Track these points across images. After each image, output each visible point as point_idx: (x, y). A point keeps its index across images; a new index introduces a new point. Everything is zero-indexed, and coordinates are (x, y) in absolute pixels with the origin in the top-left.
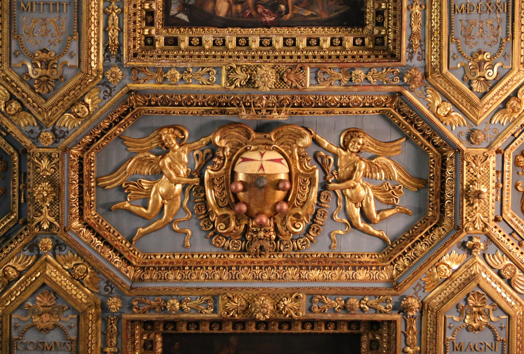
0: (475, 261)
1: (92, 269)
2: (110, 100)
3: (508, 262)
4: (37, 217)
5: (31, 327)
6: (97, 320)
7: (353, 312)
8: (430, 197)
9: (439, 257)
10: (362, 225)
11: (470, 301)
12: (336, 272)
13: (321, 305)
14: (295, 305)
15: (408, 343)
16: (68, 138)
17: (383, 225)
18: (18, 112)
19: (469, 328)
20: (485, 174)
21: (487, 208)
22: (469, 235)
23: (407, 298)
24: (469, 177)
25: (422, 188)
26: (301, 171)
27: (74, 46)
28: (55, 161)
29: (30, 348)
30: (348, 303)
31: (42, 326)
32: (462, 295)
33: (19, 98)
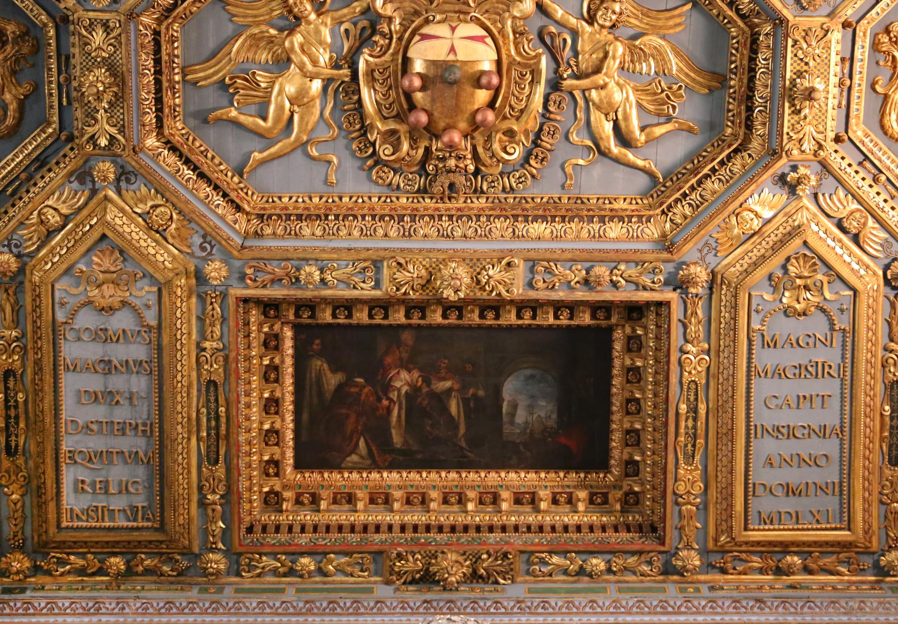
0: (801, 204)
1: (180, 213)
3: (855, 206)
4: (89, 126)
5: (84, 305)
6: (189, 297)
7: (599, 288)
8: (729, 103)
9: (741, 199)
10: (616, 149)
11: (791, 268)
12: (573, 225)
13: (547, 277)
14: (506, 276)
15: (688, 337)
17: (650, 151)
19: (787, 312)
20: (823, 61)
21: (823, 117)
22: (792, 163)
23: (688, 265)
24: (795, 65)
25: (717, 88)
26: (518, 59)
29: (85, 337)
30: (592, 273)
31: (104, 303)
32: (779, 259)
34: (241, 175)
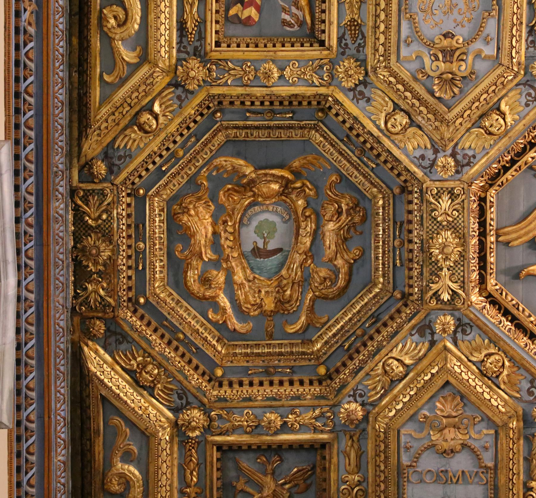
4: (433, 283)
5: (427, 449)
6: (519, 439)
16: (475, 165)
28: (459, 200)
29: (428, 479)
31: (446, 446)
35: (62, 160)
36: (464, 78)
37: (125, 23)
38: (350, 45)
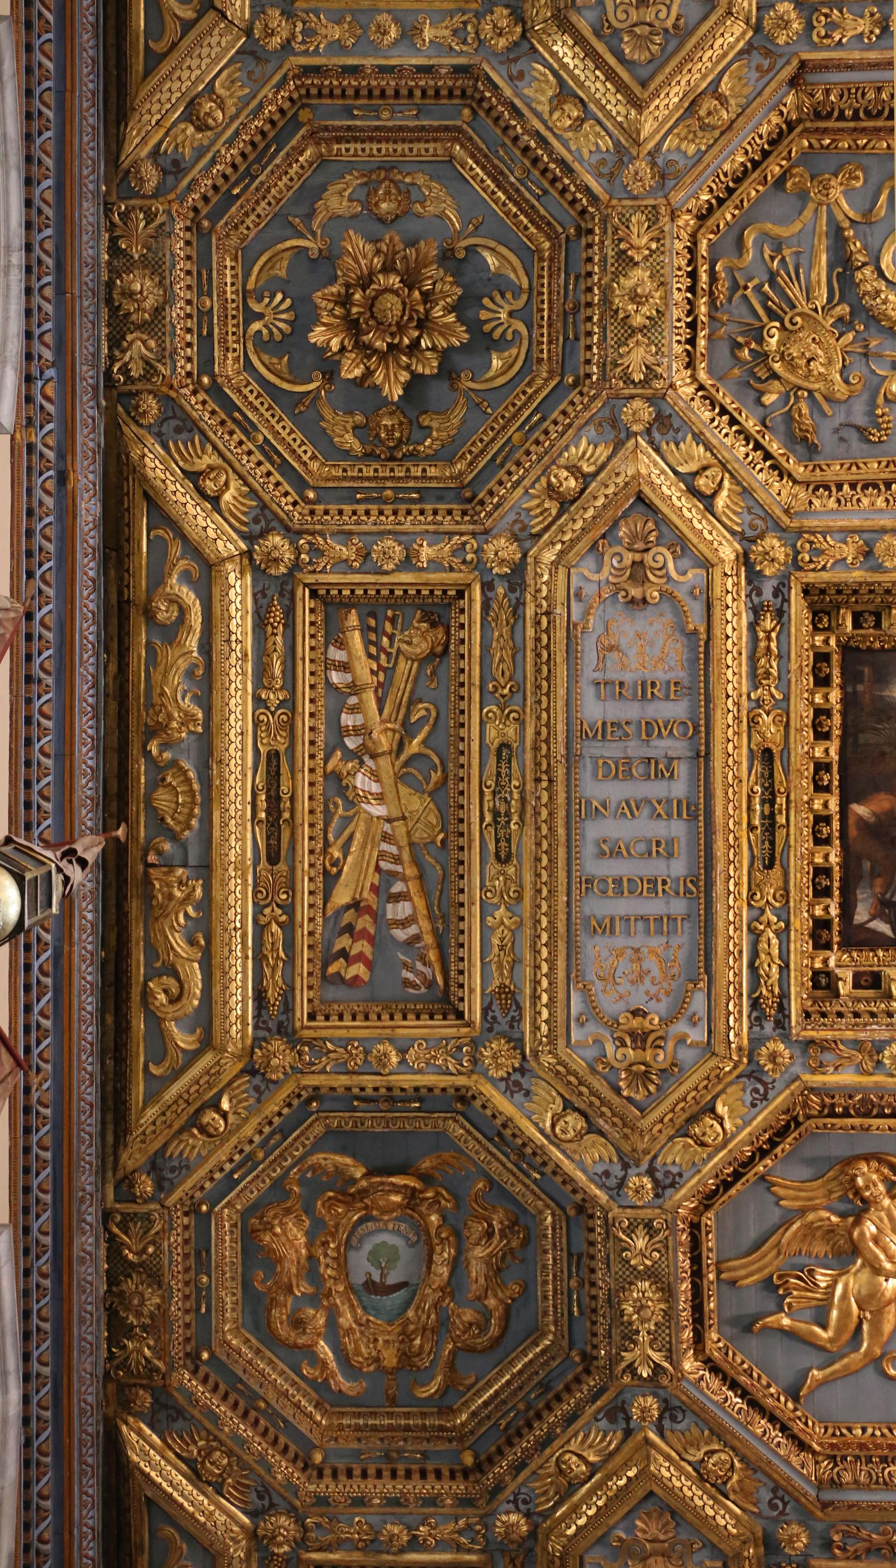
1: (741, 1461)
2: (766, 1107)
16: (682, 1186)
18: (580, 1136)
27: (698, 1003)
33: (583, 1106)
34: (796, 1399)
35: (92, 1179)
36: (663, 1071)
37: (179, 998)
38: (499, 1019)
